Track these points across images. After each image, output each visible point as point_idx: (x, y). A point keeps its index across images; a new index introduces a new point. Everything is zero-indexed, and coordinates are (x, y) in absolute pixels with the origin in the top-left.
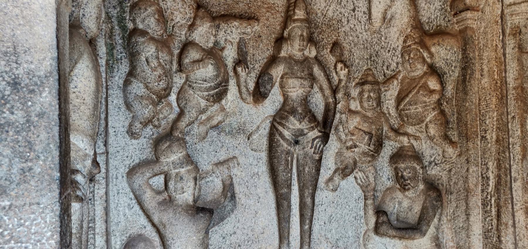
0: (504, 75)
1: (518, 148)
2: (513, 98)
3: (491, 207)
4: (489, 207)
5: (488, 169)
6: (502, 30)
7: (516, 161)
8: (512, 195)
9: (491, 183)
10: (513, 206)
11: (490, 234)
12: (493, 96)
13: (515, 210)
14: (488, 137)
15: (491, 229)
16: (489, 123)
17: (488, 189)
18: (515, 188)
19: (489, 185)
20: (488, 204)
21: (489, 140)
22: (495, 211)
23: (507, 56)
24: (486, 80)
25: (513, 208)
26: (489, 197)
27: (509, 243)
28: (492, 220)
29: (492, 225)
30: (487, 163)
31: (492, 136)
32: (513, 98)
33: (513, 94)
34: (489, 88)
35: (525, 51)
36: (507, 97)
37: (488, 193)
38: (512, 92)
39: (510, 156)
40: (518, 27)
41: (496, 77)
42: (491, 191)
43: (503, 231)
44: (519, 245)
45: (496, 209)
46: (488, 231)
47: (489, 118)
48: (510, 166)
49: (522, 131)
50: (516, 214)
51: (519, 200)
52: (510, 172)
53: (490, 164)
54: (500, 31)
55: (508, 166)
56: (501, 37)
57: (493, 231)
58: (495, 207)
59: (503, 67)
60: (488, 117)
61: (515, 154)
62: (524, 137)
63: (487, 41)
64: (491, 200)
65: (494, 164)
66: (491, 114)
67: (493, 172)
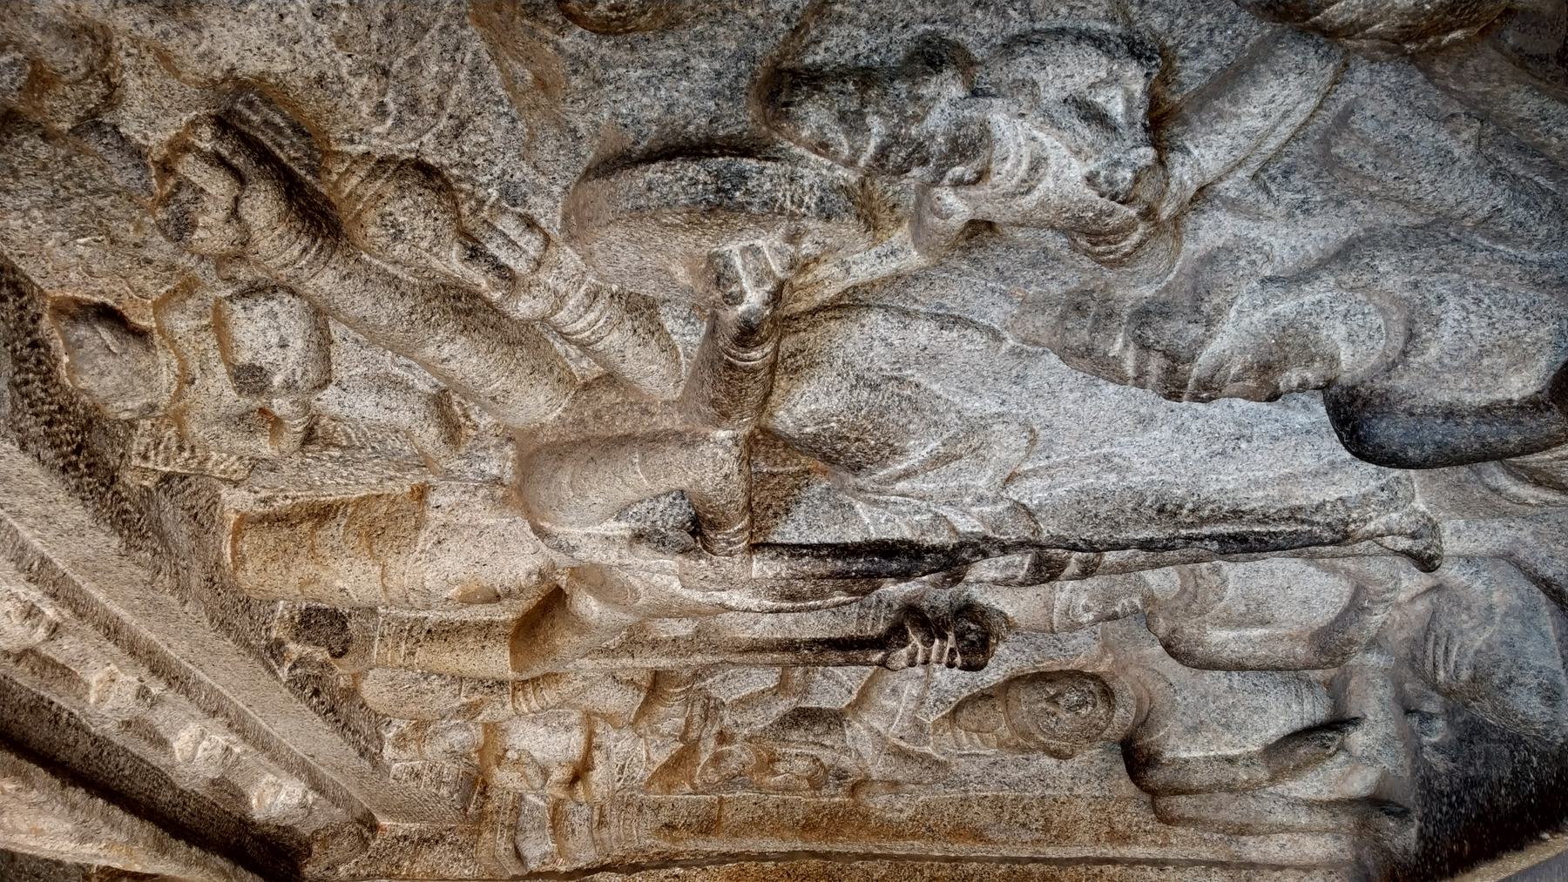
0: (769, 865)
6: (659, 867)
23: (725, 850)
35: (715, 812)
36: (826, 856)
39: (977, 859)
40: (658, 831)
48: (1004, 860)
49: (914, 836)
52: (1017, 860)
54: (662, 873)
56: (678, 871)
59: (751, 866)
62: (929, 829)
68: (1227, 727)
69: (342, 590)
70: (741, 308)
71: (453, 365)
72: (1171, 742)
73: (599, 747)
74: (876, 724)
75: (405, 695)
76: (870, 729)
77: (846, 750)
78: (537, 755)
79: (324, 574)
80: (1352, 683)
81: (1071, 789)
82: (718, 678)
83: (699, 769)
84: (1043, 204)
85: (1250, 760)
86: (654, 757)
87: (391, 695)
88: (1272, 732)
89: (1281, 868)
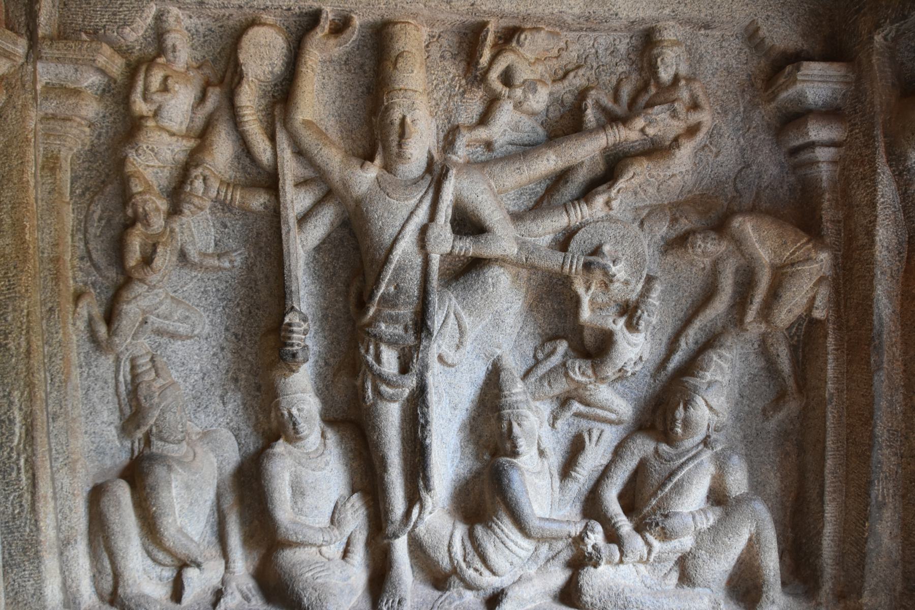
1: (59, 362)
2: (49, 277)
3: (19, 473)
4: (14, 474)
5: (11, 403)
7: (57, 385)
8: (49, 444)
9: (17, 430)
10: (51, 463)
11: (18, 523)
12: (22, 271)
13: (55, 469)
14: (12, 345)
15: (19, 513)
16: (14, 319)
17: (12, 441)
18: (55, 432)
19: (13, 434)
20: (13, 469)
21: (13, 351)
22: (28, 479)
24: (8, 241)
25: (51, 467)
26: (14, 455)
27: (50, 529)
28: (20, 496)
29: (21, 506)
30: (10, 393)
31: (19, 344)
32: (49, 277)
33: (49, 270)
34: (13, 255)
37: (12, 449)
38: (48, 267)
39: (45, 377)
41: (27, 237)
42: (19, 444)
43: (42, 510)
44: (63, 528)
45: (29, 475)
46: (14, 518)
47: (14, 310)
49: (64, 334)
50: (56, 476)
51: (61, 451)
52: (47, 405)
53: (16, 393)
55: (43, 395)
57: (24, 515)
58: (27, 471)
60: (10, 308)
61: (55, 373)
63: (11, 170)
64: (18, 459)
65: (22, 394)
66: (17, 303)
67: (21, 409)
68: (191, 504)
69: (412, 71)
70: (611, 265)
71: (545, 162)
72: (179, 477)
73: (177, 141)
74: (163, 307)
75: (262, 50)
76: (161, 303)
77: (152, 288)
78: (173, 102)
79: (418, 66)
80: (212, 563)
81: (86, 433)
82: (209, 216)
83: (154, 198)
84: (624, 348)
85: (175, 520)
86: (150, 170)
87: (263, 42)
88: (189, 529)
89: (62, 572)
